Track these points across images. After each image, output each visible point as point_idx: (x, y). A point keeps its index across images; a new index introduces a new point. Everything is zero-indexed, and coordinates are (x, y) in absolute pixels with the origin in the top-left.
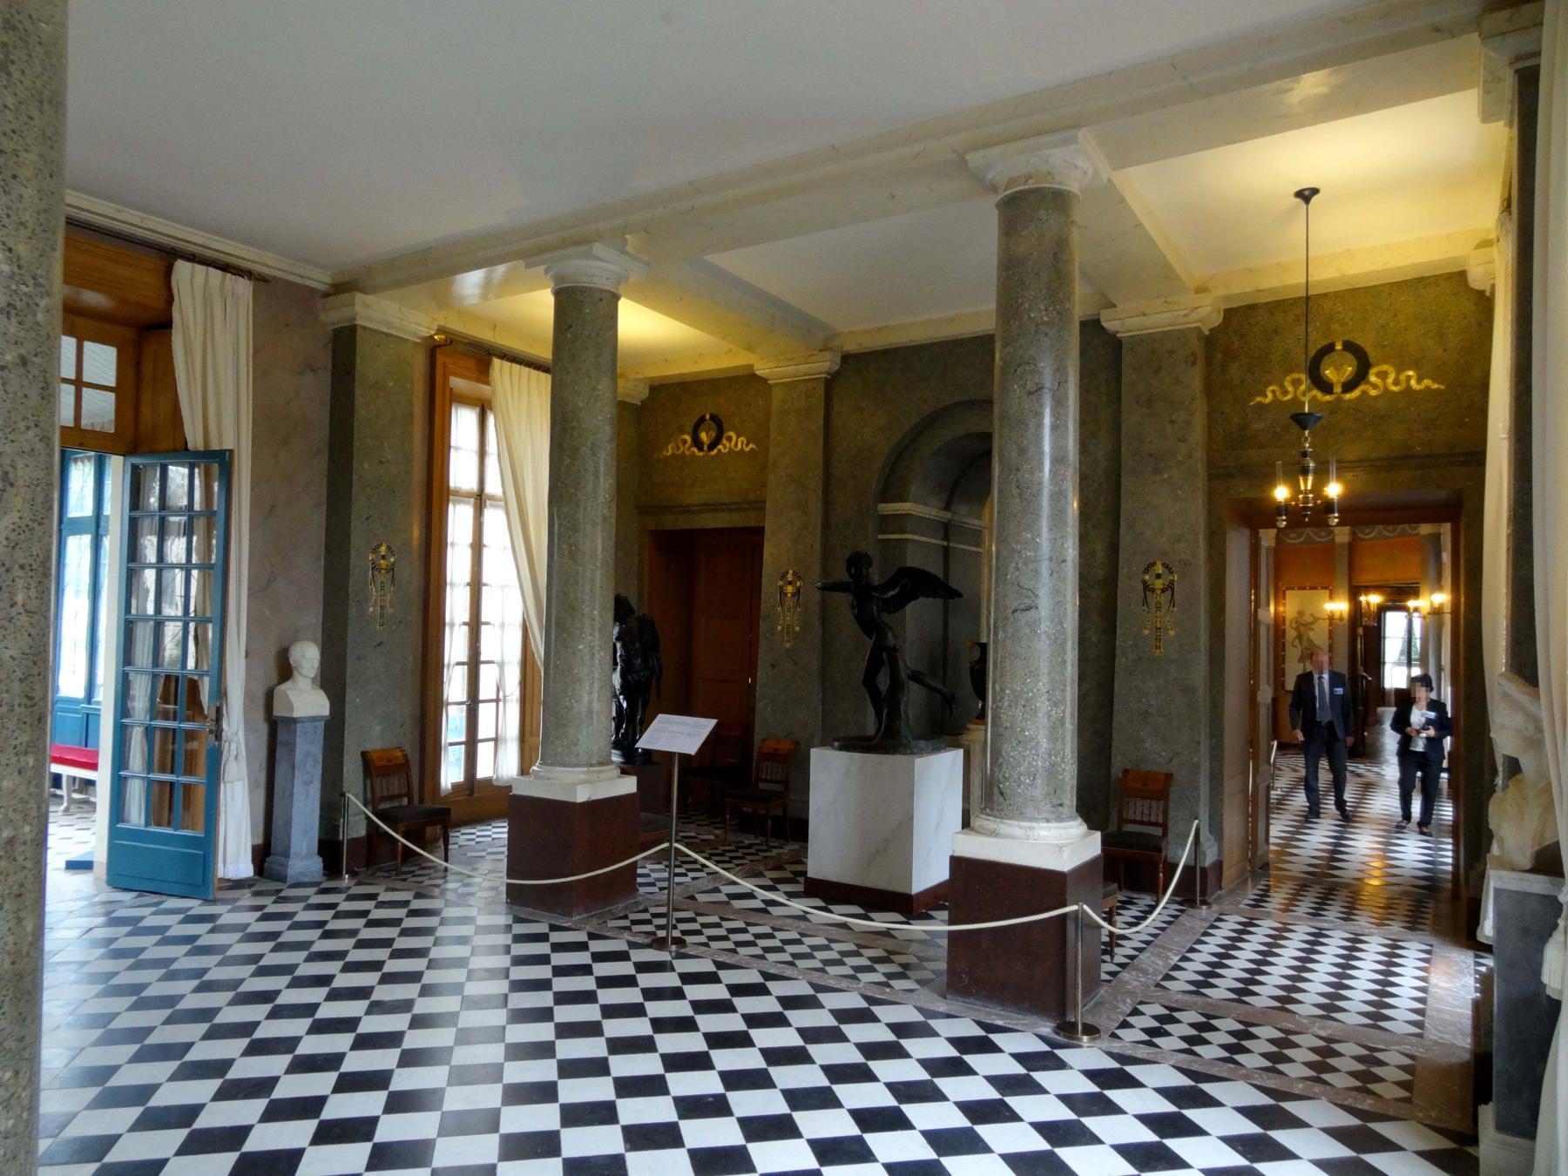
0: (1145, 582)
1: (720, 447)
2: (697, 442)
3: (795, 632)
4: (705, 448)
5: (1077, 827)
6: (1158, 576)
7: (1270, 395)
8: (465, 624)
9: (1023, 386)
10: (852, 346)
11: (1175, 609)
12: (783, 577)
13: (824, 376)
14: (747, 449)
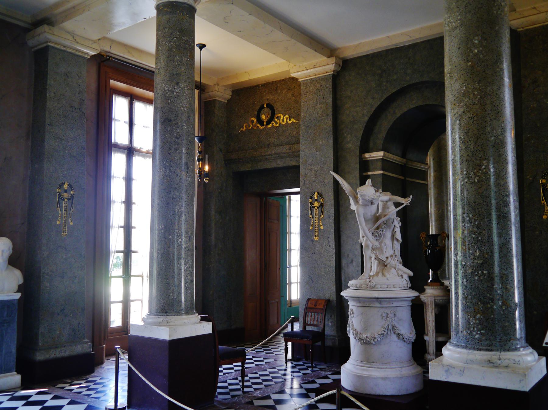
1: (273, 122)
2: (261, 122)
4: (265, 123)
8: (121, 227)
10: (350, 54)
12: (312, 198)
14: (289, 122)
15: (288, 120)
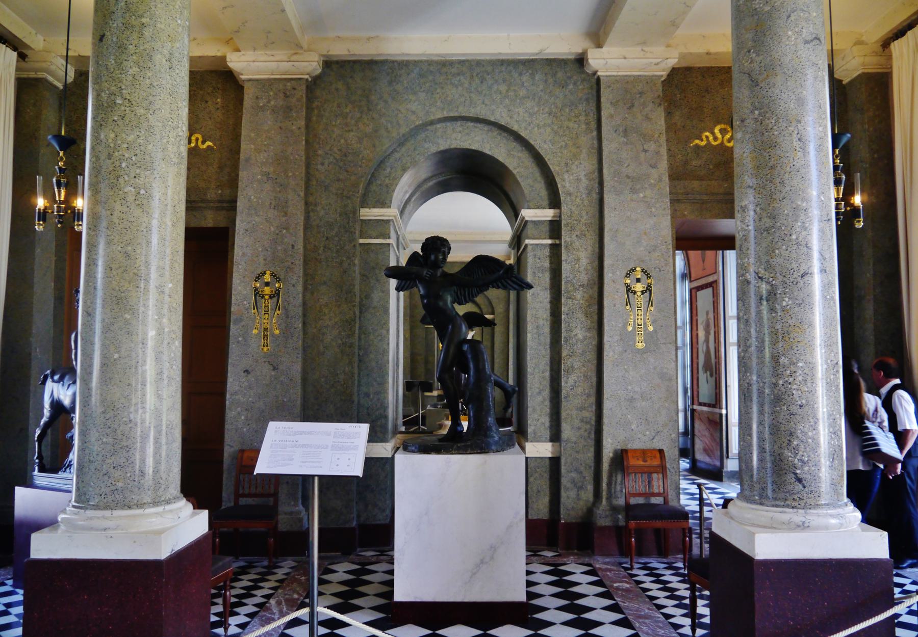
3: (273, 335)
7: (704, 139)
9: (799, 33)
11: (652, 309)
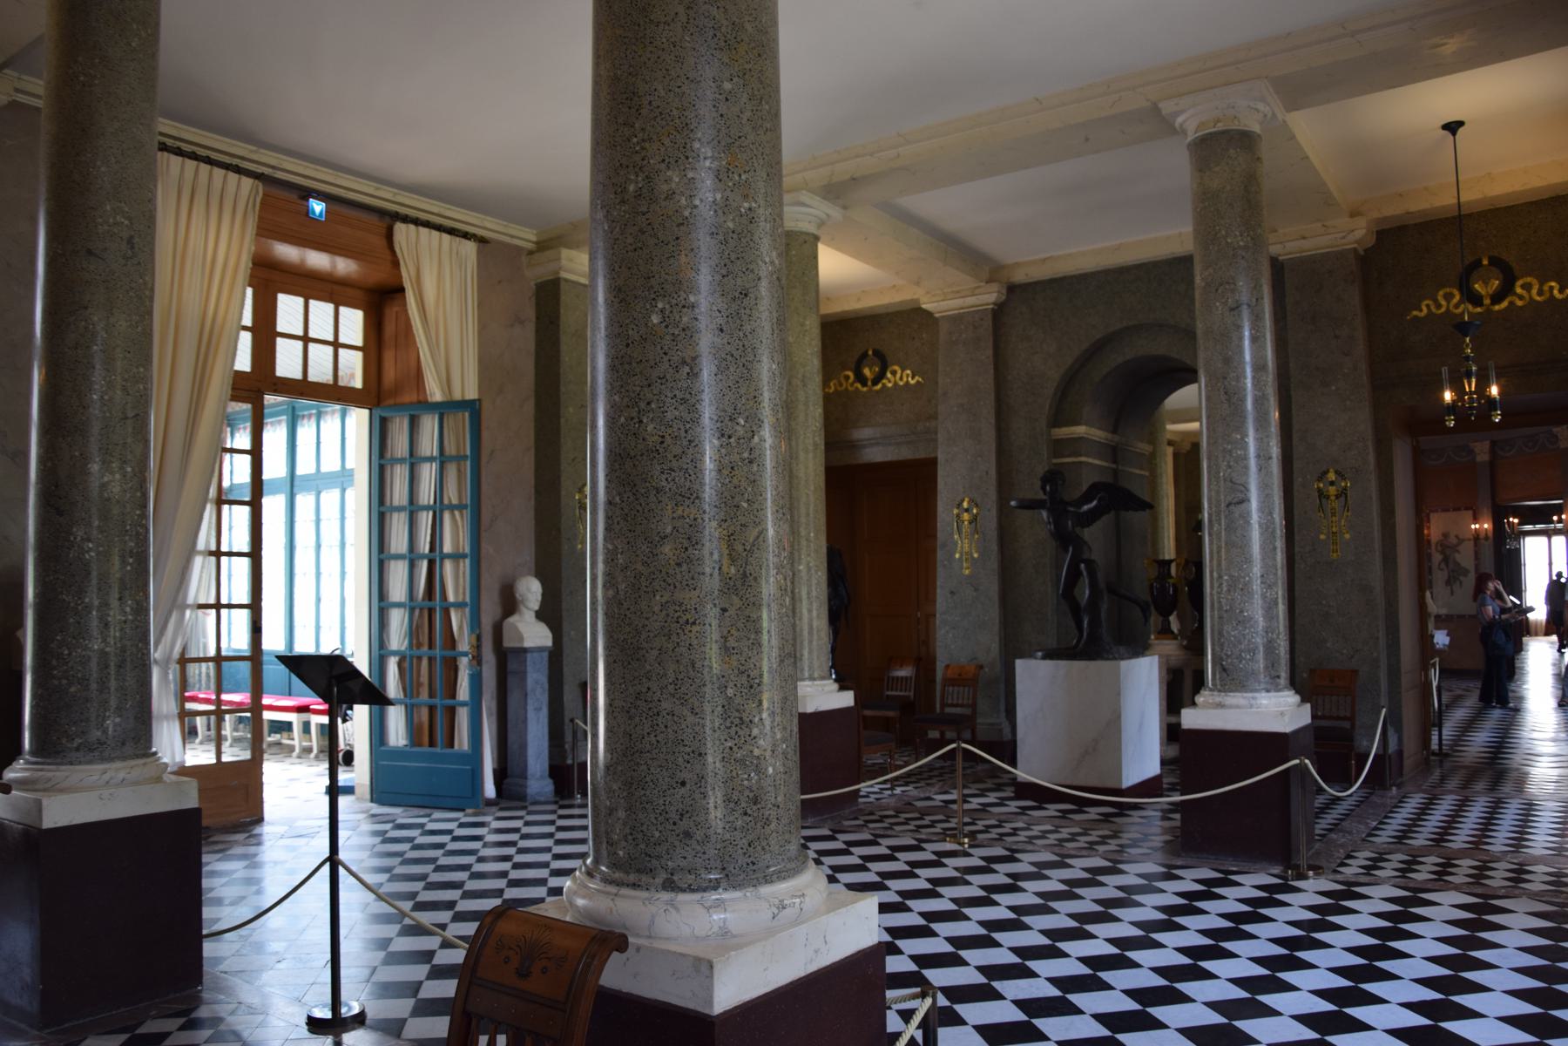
0: (1319, 490)
1: (884, 381)
2: (861, 379)
5: (1290, 698)
6: (1332, 483)
7: (1425, 309)
9: (1225, 303)
10: (1019, 277)
11: (1349, 514)
12: (959, 505)
13: (991, 306)
15: (910, 379)
